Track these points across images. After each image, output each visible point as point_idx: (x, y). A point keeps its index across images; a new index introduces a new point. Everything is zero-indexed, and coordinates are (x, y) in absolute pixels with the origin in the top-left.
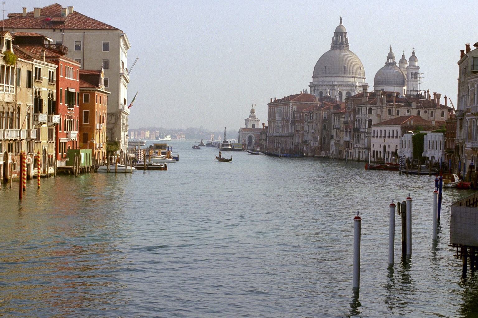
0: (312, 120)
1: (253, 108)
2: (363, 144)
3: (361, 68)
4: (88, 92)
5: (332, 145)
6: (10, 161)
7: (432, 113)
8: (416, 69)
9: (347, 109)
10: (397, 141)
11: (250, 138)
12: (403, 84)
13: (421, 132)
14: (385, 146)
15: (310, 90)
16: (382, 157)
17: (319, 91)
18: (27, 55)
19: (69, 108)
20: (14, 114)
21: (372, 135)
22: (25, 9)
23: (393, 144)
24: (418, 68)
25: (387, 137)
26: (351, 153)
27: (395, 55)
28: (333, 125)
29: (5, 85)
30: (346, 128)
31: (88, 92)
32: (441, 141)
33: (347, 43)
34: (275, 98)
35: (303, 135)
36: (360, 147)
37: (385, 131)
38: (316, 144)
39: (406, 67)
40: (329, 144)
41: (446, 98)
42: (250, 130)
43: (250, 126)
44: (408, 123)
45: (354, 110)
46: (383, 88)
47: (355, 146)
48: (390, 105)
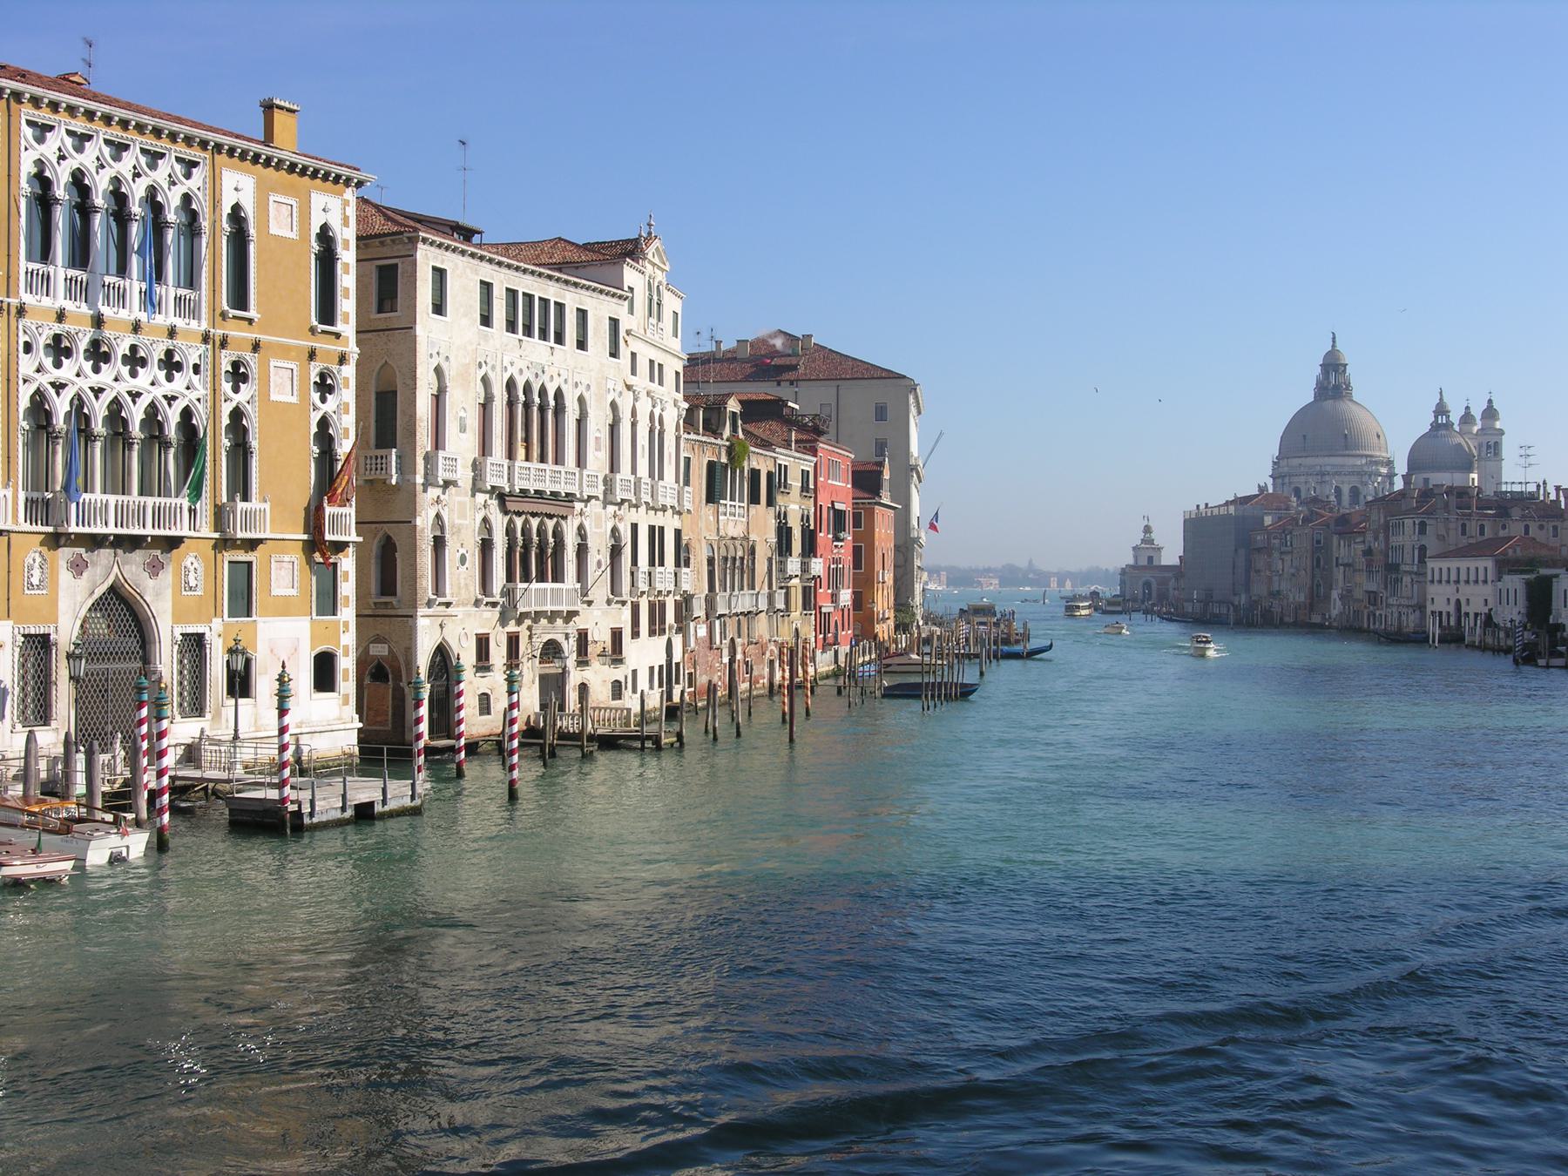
0: (1289, 549)
1: (1151, 524)
2: (1408, 598)
3: (1378, 436)
4: (861, 506)
5: (1335, 600)
6: (739, 656)
7: (1555, 528)
8: (1497, 435)
10: (1487, 591)
11: (1147, 585)
12: (1470, 469)
13: (1544, 571)
14: (1458, 602)
15: (1274, 485)
16: (1452, 623)
17: (1293, 486)
18: (762, 440)
19: (835, 543)
20: (745, 562)
21: (1429, 578)
22: (718, 343)
23: (1478, 598)
24: (1501, 432)
25: (1462, 583)
28: (1337, 558)
29: (729, 502)
30: (1369, 565)
31: (861, 506)
33: (1348, 386)
34: (1207, 505)
35: (1270, 579)
37: (1477, 569)
38: (1301, 598)
39: (1475, 431)
40: (1328, 597)
42: (1144, 568)
43: (1143, 562)
44: (1510, 551)
45: (1386, 527)
47: (1391, 601)
48: (1464, 515)
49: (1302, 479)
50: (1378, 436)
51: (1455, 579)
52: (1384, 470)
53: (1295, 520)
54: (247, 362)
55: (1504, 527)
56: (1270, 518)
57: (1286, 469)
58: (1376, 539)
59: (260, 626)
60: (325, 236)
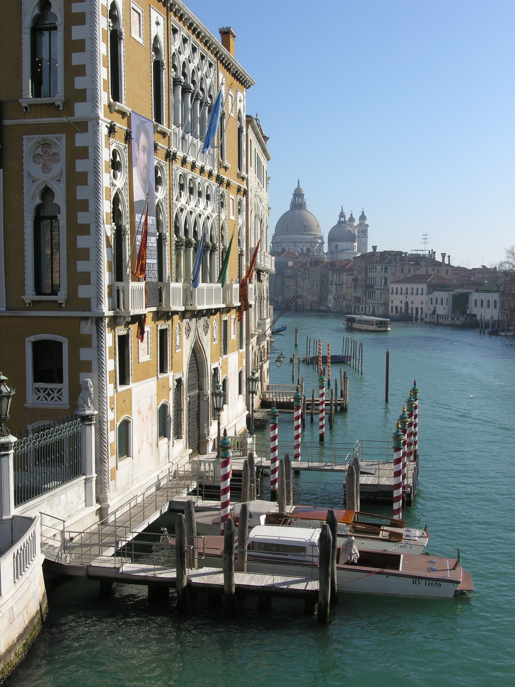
2: (379, 300)
3: (318, 226)
5: (330, 300)
7: (438, 270)
9: (356, 268)
12: (354, 241)
14: (407, 303)
15: (273, 246)
16: (403, 311)
17: (282, 247)
21: (390, 291)
24: (367, 226)
26: (362, 308)
27: (346, 215)
32: (495, 301)
33: (305, 203)
36: (375, 302)
38: (315, 299)
40: (326, 298)
41: (449, 256)
44: (433, 281)
45: (366, 269)
46: (336, 243)
47: (368, 301)
48: (402, 264)
49: (286, 244)
50: (318, 226)
51: (405, 292)
52: (320, 241)
53: (306, 264)
54: (224, 195)
55: (418, 270)
56: (291, 262)
57: (279, 240)
58: (360, 274)
59: (229, 359)
60: (239, 119)
